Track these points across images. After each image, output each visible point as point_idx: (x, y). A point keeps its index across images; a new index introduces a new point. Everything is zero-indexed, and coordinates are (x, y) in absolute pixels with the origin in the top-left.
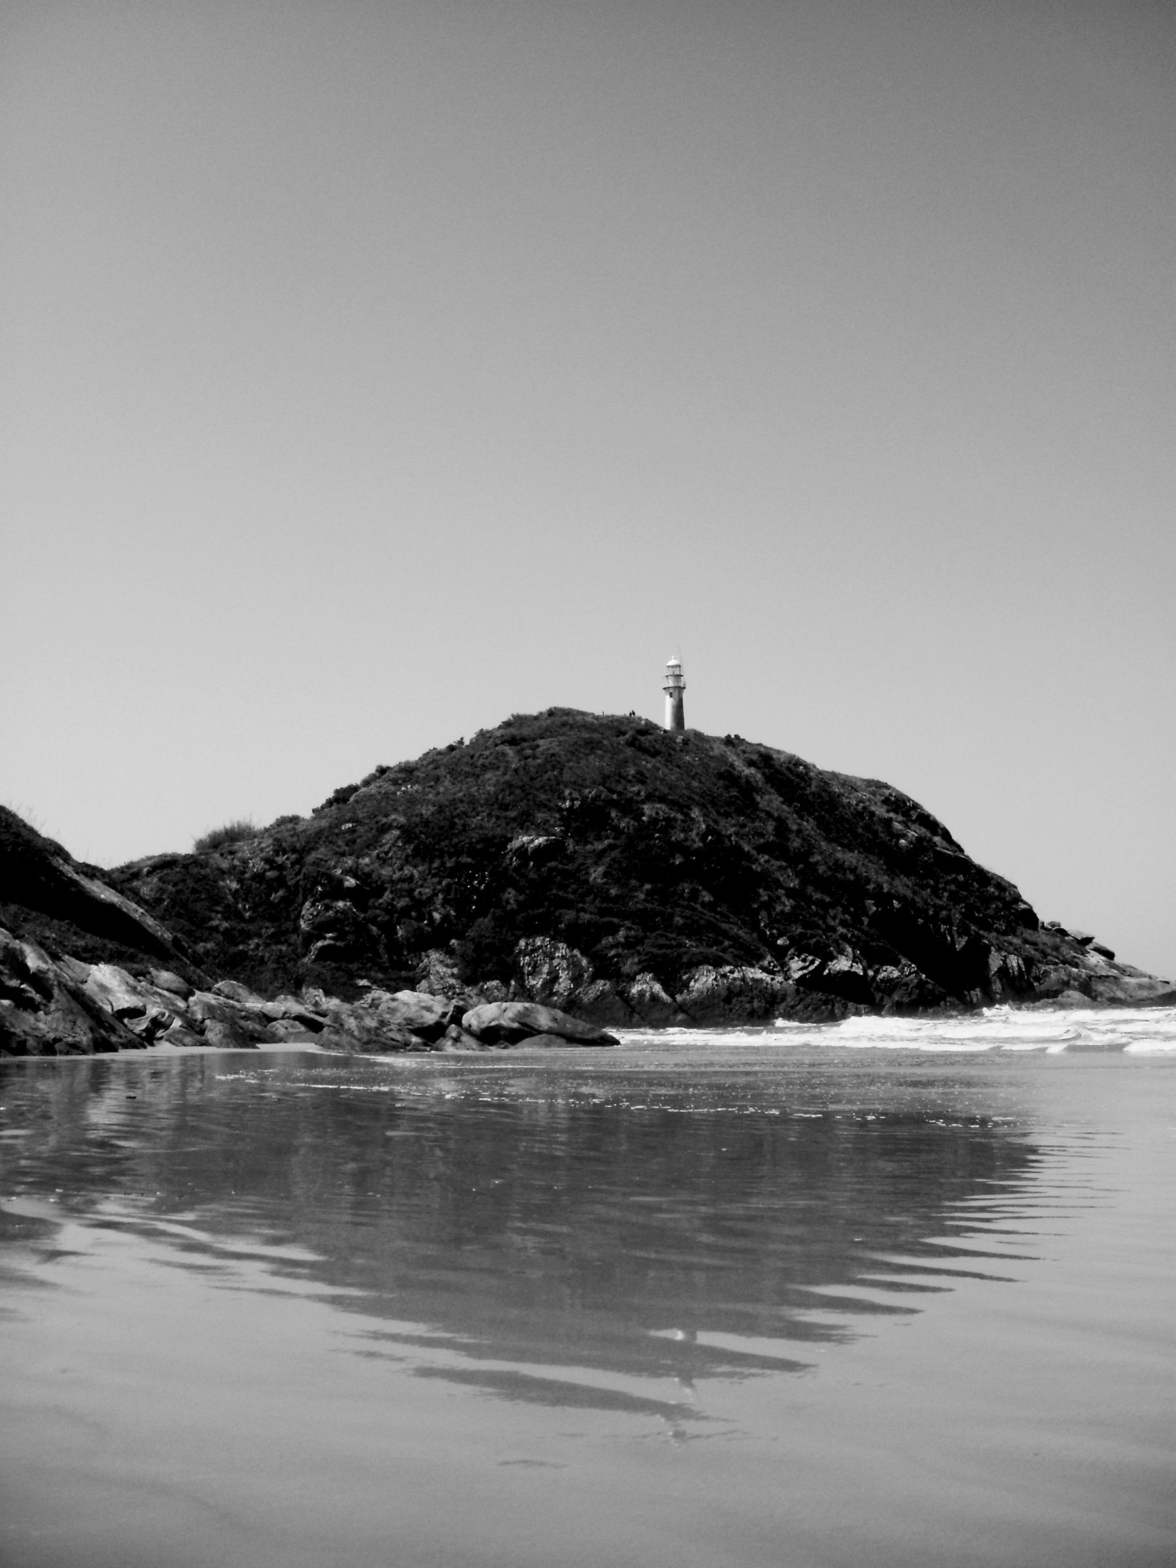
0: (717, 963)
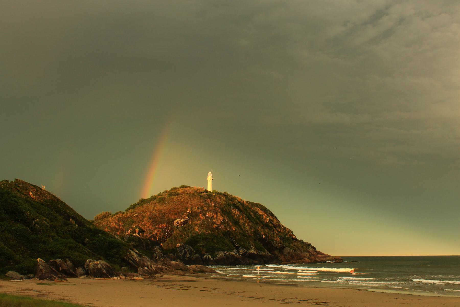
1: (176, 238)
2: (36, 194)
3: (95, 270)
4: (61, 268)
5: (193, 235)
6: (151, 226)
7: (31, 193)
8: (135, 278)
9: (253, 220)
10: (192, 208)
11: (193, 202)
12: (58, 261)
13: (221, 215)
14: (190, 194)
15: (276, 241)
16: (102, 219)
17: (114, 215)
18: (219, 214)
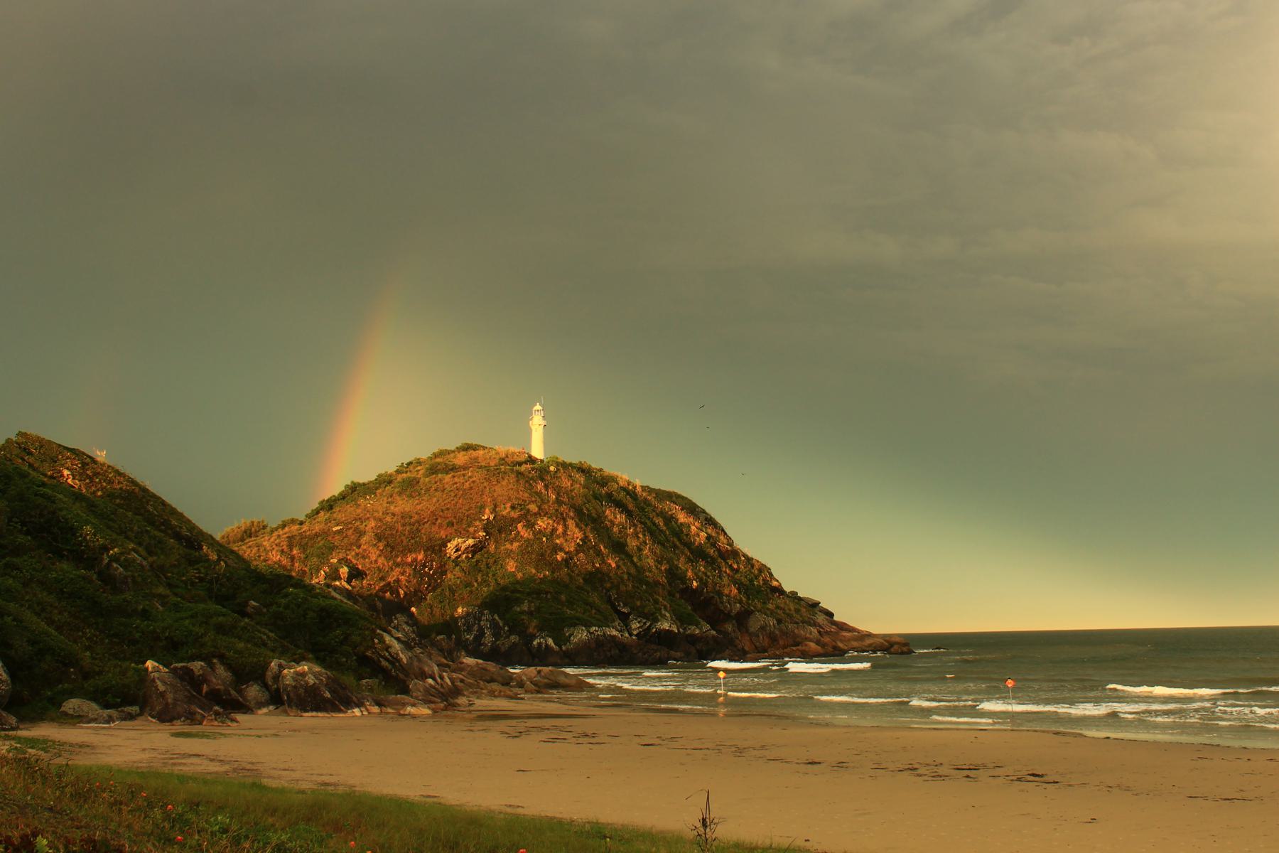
0: (588, 625)
1: (452, 591)
2: (81, 474)
3: (301, 691)
4: (205, 688)
5: (502, 582)
6: (381, 560)
7: (66, 472)
8: (409, 709)
9: (662, 538)
10: (496, 506)
11: (498, 489)
12: (197, 666)
13: (577, 526)
14: (487, 468)
15: (728, 596)
16: (242, 540)
17: (276, 529)
18: (571, 523)
